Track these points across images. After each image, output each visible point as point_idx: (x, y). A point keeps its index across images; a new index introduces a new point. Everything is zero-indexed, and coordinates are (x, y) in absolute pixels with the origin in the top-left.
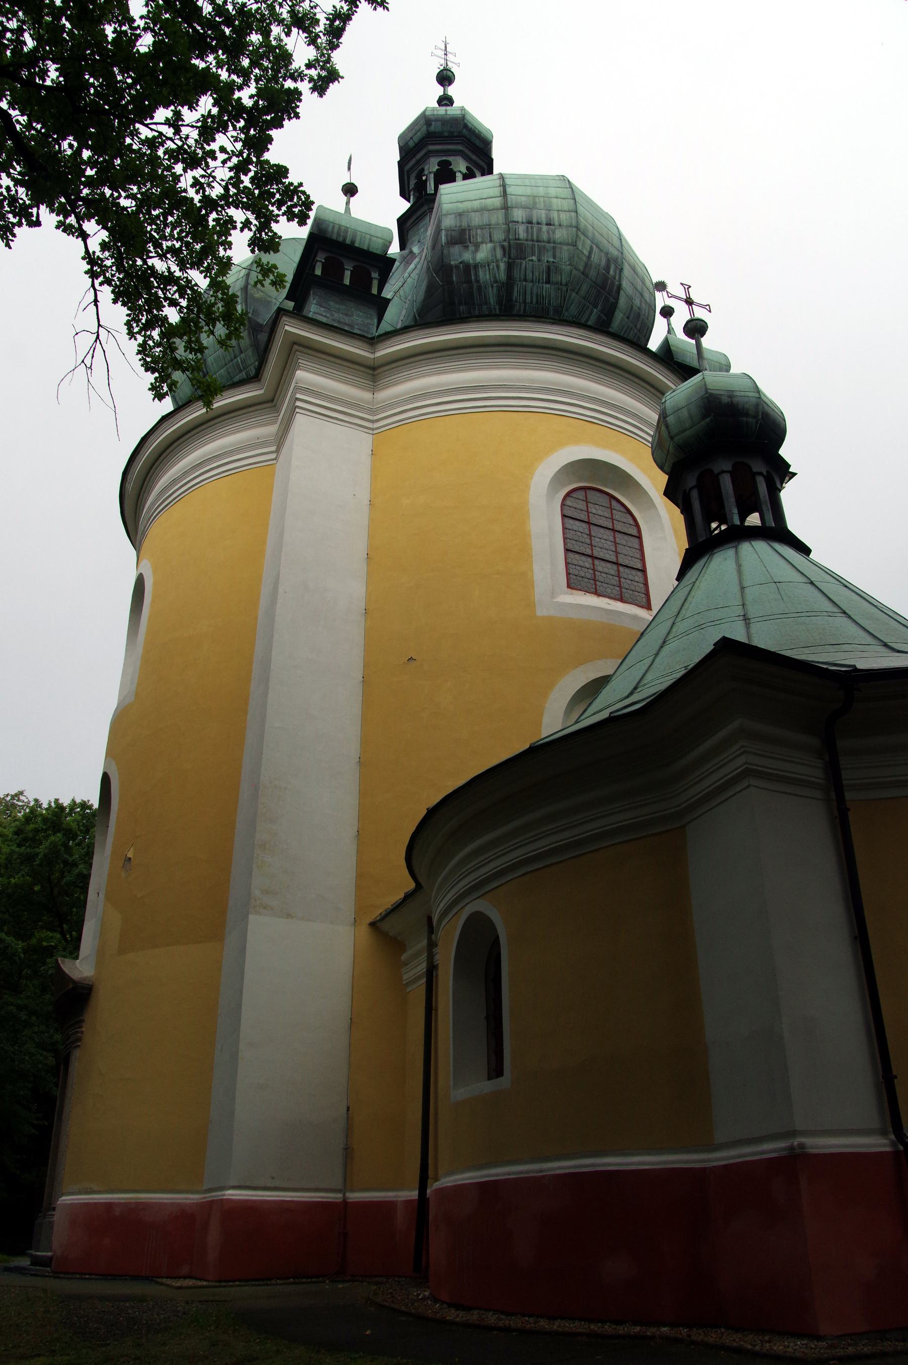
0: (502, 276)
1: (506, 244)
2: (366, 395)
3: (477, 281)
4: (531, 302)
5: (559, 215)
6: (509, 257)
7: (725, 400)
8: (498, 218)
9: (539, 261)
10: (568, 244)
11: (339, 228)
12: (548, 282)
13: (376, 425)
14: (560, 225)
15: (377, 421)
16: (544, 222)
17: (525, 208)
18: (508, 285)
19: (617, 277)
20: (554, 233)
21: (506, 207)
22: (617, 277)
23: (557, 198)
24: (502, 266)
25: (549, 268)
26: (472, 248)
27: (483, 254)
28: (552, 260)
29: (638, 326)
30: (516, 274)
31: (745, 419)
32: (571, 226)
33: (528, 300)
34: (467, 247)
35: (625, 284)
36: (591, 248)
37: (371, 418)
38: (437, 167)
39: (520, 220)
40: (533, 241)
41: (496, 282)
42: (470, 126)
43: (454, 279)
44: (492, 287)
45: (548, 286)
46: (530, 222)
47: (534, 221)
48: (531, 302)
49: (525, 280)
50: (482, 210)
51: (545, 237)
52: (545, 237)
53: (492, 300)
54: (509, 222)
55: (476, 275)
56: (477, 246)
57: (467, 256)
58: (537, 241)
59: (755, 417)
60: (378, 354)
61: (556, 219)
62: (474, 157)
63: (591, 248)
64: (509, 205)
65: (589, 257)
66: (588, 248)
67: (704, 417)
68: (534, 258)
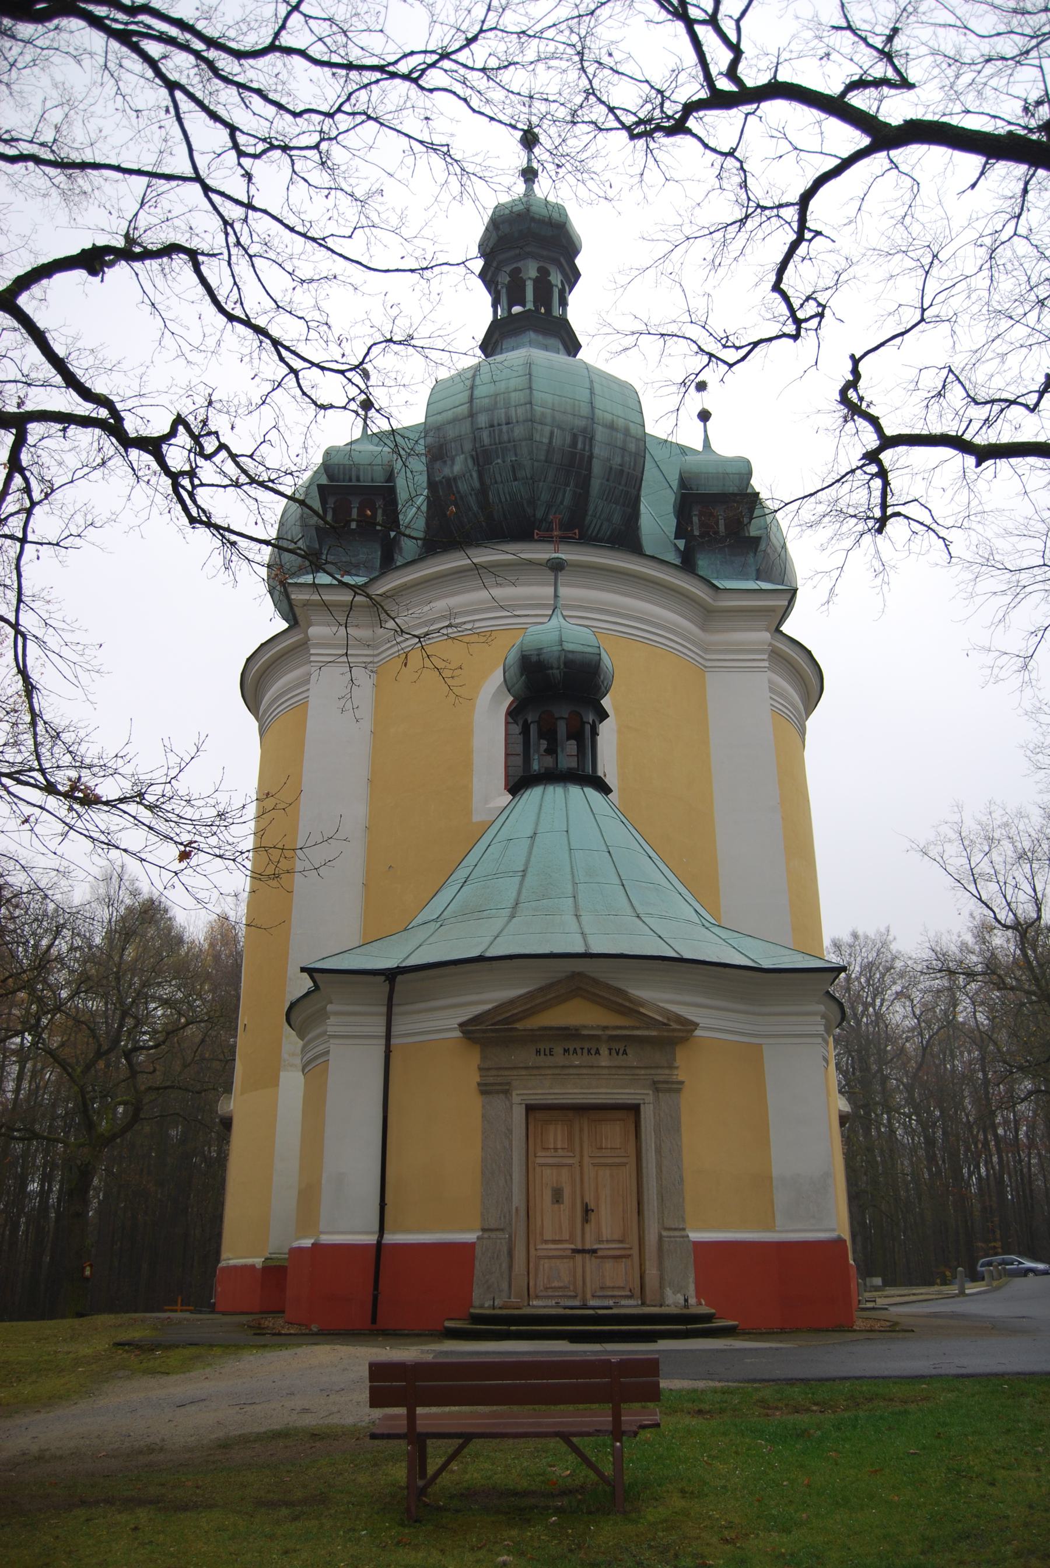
0: (476, 484)
3: (459, 492)
6: (478, 465)
7: (534, 659)
8: (465, 428)
10: (526, 439)
11: (344, 468)
12: (515, 479)
16: (504, 422)
17: (487, 410)
18: (483, 491)
19: (587, 448)
20: (512, 431)
21: (472, 415)
22: (587, 448)
23: (515, 390)
24: (475, 475)
25: (513, 466)
26: (449, 462)
27: (458, 467)
29: (623, 482)
30: (488, 481)
33: (503, 500)
34: (445, 462)
35: (596, 451)
36: (552, 433)
37: (376, 652)
38: (508, 279)
39: (483, 426)
41: (473, 489)
42: (537, 217)
46: (492, 426)
47: (496, 423)
50: (455, 420)
51: (505, 438)
52: (505, 438)
53: (475, 508)
54: (476, 430)
55: (457, 487)
57: (446, 471)
59: (558, 668)
62: (545, 253)
63: (552, 433)
65: (550, 442)
66: (547, 434)
67: (522, 675)
68: (499, 461)
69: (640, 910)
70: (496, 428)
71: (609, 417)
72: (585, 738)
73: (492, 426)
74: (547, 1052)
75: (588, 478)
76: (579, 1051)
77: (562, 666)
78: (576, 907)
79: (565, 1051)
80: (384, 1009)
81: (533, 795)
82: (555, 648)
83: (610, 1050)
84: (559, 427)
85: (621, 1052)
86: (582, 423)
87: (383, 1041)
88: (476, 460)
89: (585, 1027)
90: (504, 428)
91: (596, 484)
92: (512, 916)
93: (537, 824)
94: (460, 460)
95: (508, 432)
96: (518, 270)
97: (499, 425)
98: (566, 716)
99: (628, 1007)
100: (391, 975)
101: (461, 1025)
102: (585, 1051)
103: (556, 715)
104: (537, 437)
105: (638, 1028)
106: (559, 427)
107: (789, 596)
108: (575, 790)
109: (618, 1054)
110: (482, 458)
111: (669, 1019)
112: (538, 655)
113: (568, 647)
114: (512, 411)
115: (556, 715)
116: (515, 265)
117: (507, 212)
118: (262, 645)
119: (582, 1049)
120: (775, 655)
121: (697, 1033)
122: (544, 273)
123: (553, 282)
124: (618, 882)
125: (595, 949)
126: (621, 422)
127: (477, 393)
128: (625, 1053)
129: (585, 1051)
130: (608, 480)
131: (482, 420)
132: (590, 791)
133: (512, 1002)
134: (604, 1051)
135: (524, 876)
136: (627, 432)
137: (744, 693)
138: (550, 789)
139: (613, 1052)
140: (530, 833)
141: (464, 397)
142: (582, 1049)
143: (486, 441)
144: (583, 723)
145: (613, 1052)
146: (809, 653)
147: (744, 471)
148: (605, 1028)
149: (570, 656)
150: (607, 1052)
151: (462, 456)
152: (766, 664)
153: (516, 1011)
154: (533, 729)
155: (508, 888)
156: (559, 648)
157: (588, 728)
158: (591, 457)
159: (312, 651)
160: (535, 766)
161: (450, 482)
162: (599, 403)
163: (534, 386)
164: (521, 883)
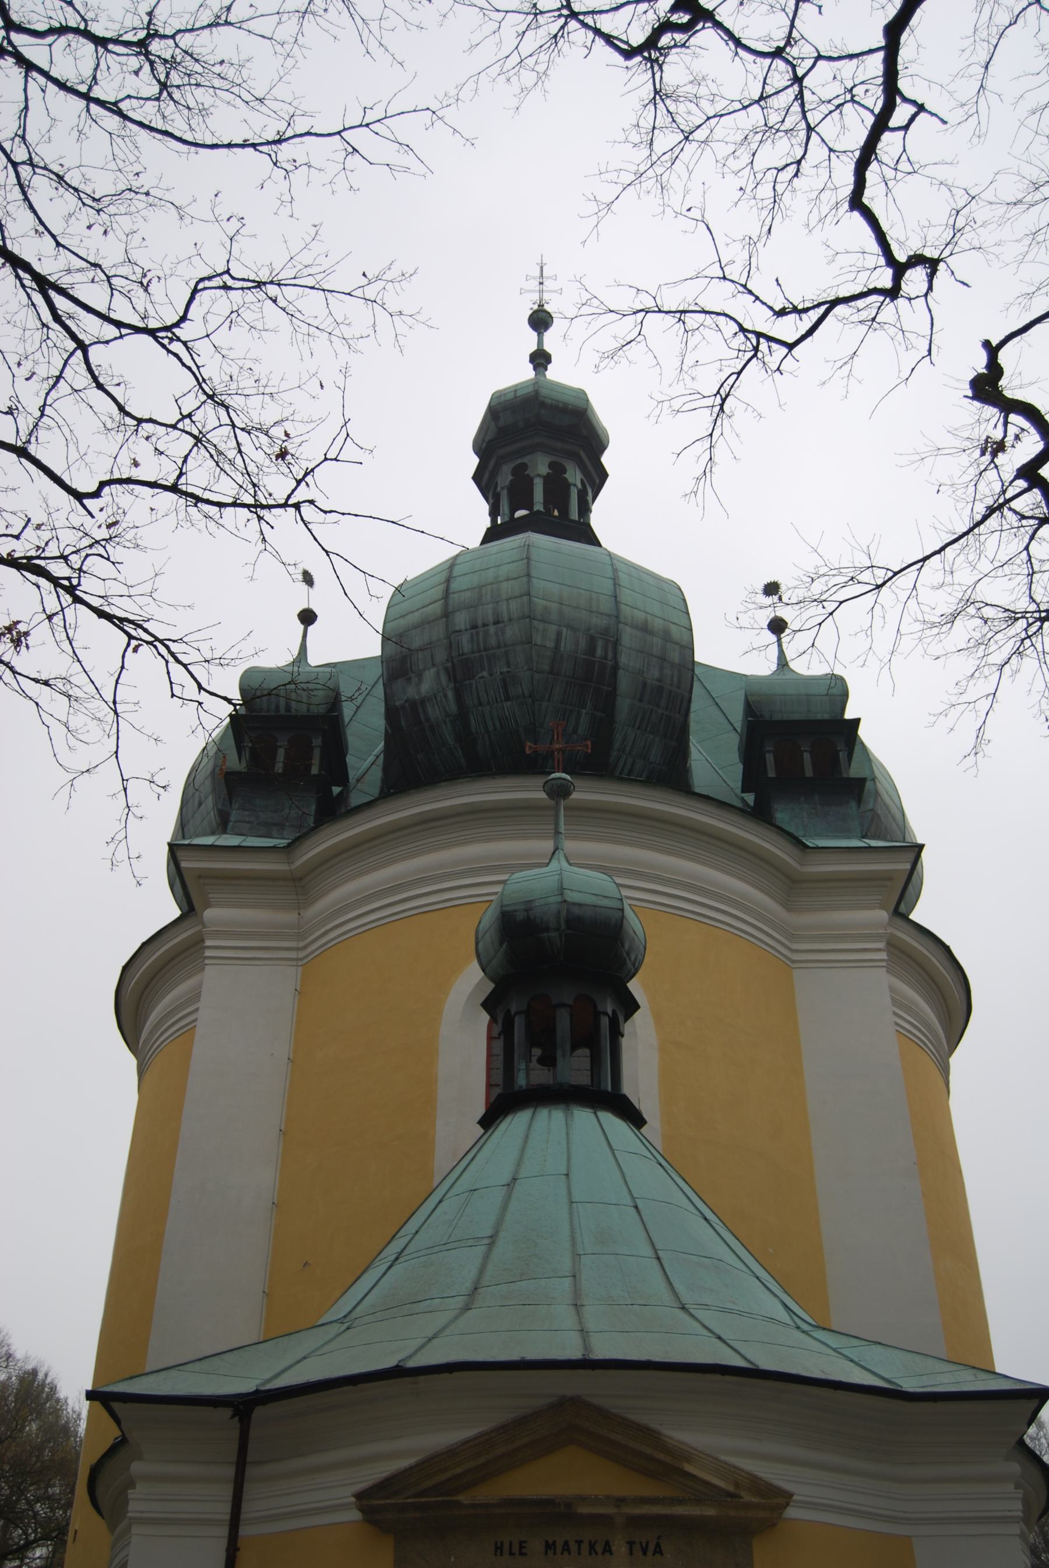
0: (453, 707)
1: (449, 665)
2: (288, 917)
3: (428, 720)
4: (495, 729)
5: (508, 605)
6: (455, 681)
7: (521, 916)
8: (438, 632)
9: (491, 675)
12: (508, 698)
13: (301, 955)
14: (510, 620)
15: (305, 947)
16: (491, 620)
19: (610, 655)
21: (447, 614)
22: (610, 655)
23: (508, 580)
24: (450, 694)
25: (504, 680)
26: (415, 680)
27: (427, 686)
28: (505, 670)
31: (545, 935)
32: (523, 617)
33: (491, 728)
34: (409, 679)
35: (623, 660)
36: (559, 634)
37: (301, 944)
38: (510, 478)
39: (463, 627)
40: (479, 651)
42: (549, 402)
43: (403, 724)
44: (445, 722)
45: (509, 703)
47: (480, 623)
48: (495, 729)
49: (480, 704)
50: (425, 623)
51: (493, 642)
52: (493, 642)
53: (450, 740)
56: (420, 676)
57: (412, 692)
58: (485, 650)
59: (557, 929)
60: (299, 862)
61: (505, 613)
62: (559, 445)
63: (559, 634)
64: (450, 609)
66: (553, 636)
67: (501, 943)
69: (687, 1297)
70: (481, 630)
71: (640, 616)
72: (601, 1038)
73: (474, 627)
74: (516, 1549)
75: (611, 698)
76: (573, 1547)
77: (563, 926)
78: (577, 1291)
79: (549, 1546)
80: (230, 1471)
81: (515, 1124)
82: (552, 900)
83: (631, 1544)
84: (569, 627)
85: (651, 1548)
86: (604, 622)
87: (225, 1531)
88: (451, 674)
89: (583, 1499)
90: (492, 629)
91: (624, 706)
92: (467, 1308)
93: (519, 1164)
94: (429, 675)
95: (496, 634)
96: (524, 467)
97: (484, 625)
98: (571, 1002)
99: (661, 1462)
100: (243, 1406)
101: (360, 1496)
102: (585, 1547)
103: (559, 1003)
104: (538, 639)
105: (680, 1502)
106: (569, 627)
107: (911, 856)
108: (583, 1116)
109: (645, 1553)
110: (460, 671)
111: (737, 1485)
112: (527, 911)
113: (572, 897)
114: (503, 607)
115: (559, 1003)
116: (519, 461)
117: (511, 396)
118: (144, 944)
119: (579, 1543)
120: (894, 947)
121: (791, 1512)
122: (557, 472)
123: (571, 480)
124: (650, 1253)
125: (603, 1350)
126: (658, 624)
127: (455, 586)
128: (658, 1550)
129: (585, 1547)
130: (641, 700)
131: (461, 620)
132: (608, 1118)
133: (452, 1453)
134: (620, 1547)
135: (491, 1245)
136: (667, 636)
137: (853, 1004)
138: (543, 1113)
139: (637, 1548)
140: (506, 1178)
141: (438, 592)
142: (579, 1543)
143: (466, 647)
144: (597, 1014)
145: (637, 1548)
146: (947, 949)
147: (836, 690)
148: (621, 1501)
149: (576, 911)
150: (624, 1549)
151: (433, 670)
152: (884, 964)
153: (459, 1470)
154: (519, 1024)
155: (465, 1264)
156: (559, 899)
157: (605, 1021)
158: (616, 667)
159: (208, 943)
160: (521, 1081)
161: (416, 706)
162: (626, 596)
163: (534, 573)
164: (486, 1257)
